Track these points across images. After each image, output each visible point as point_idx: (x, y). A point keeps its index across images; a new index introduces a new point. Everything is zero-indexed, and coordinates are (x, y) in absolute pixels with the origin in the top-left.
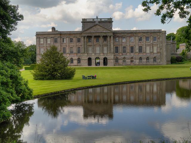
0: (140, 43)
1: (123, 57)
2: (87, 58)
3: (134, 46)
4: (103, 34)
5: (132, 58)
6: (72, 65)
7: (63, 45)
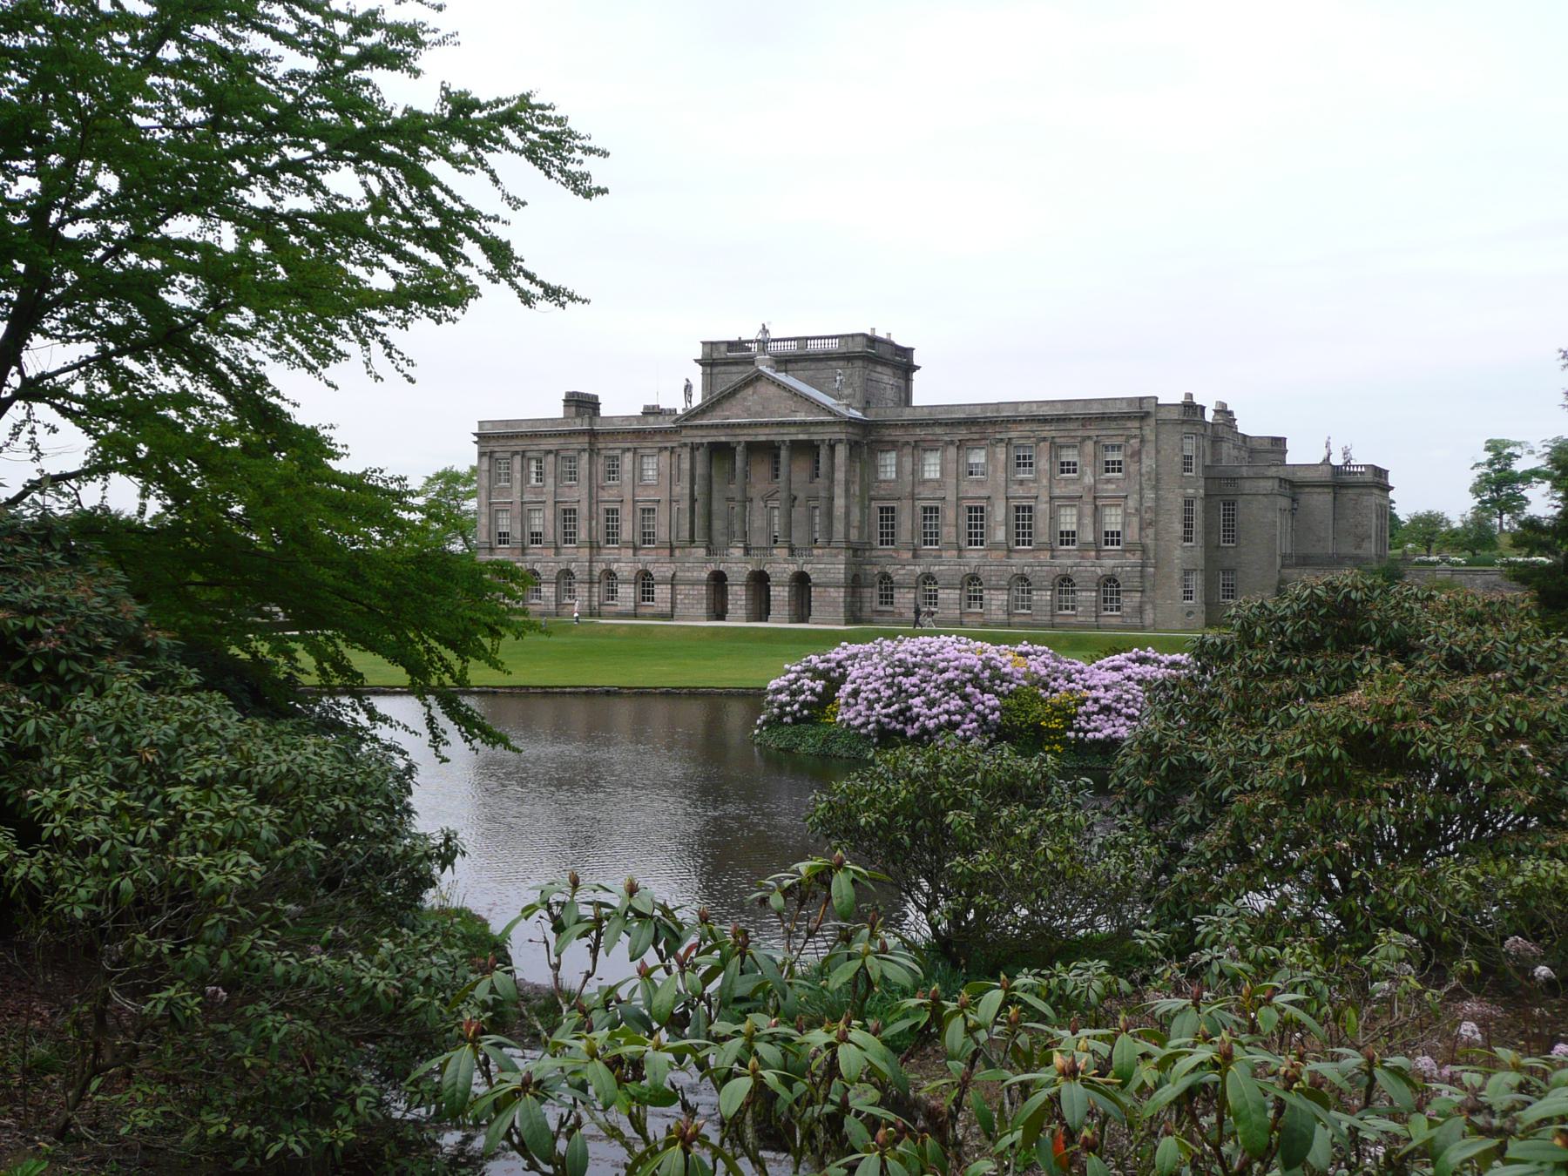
0: (1021, 482)
1: (919, 570)
2: (705, 575)
3: (983, 503)
4: (793, 430)
5: (973, 579)
6: (649, 610)
7: (604, 495)
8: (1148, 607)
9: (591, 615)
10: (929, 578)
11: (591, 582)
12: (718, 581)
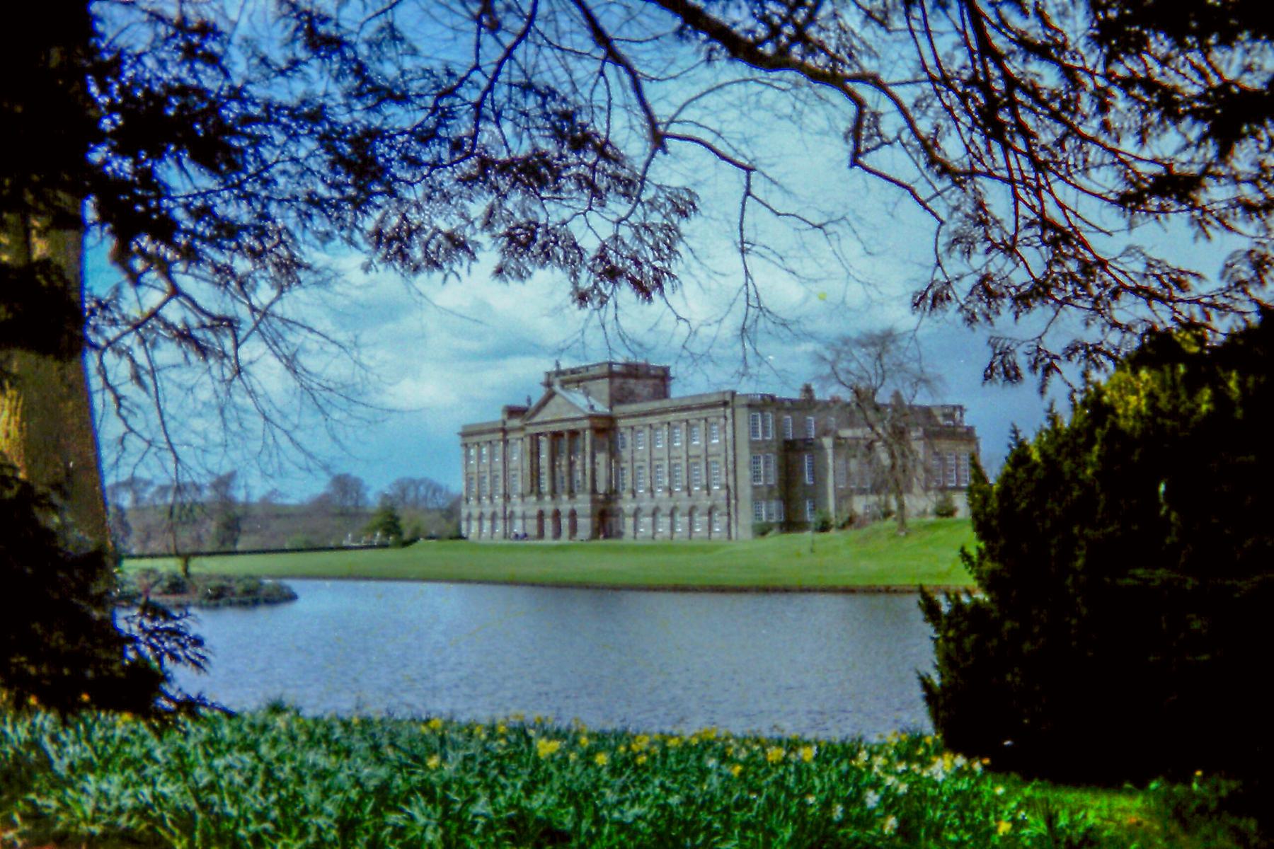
8: (733, 525)
12: (541, 516)
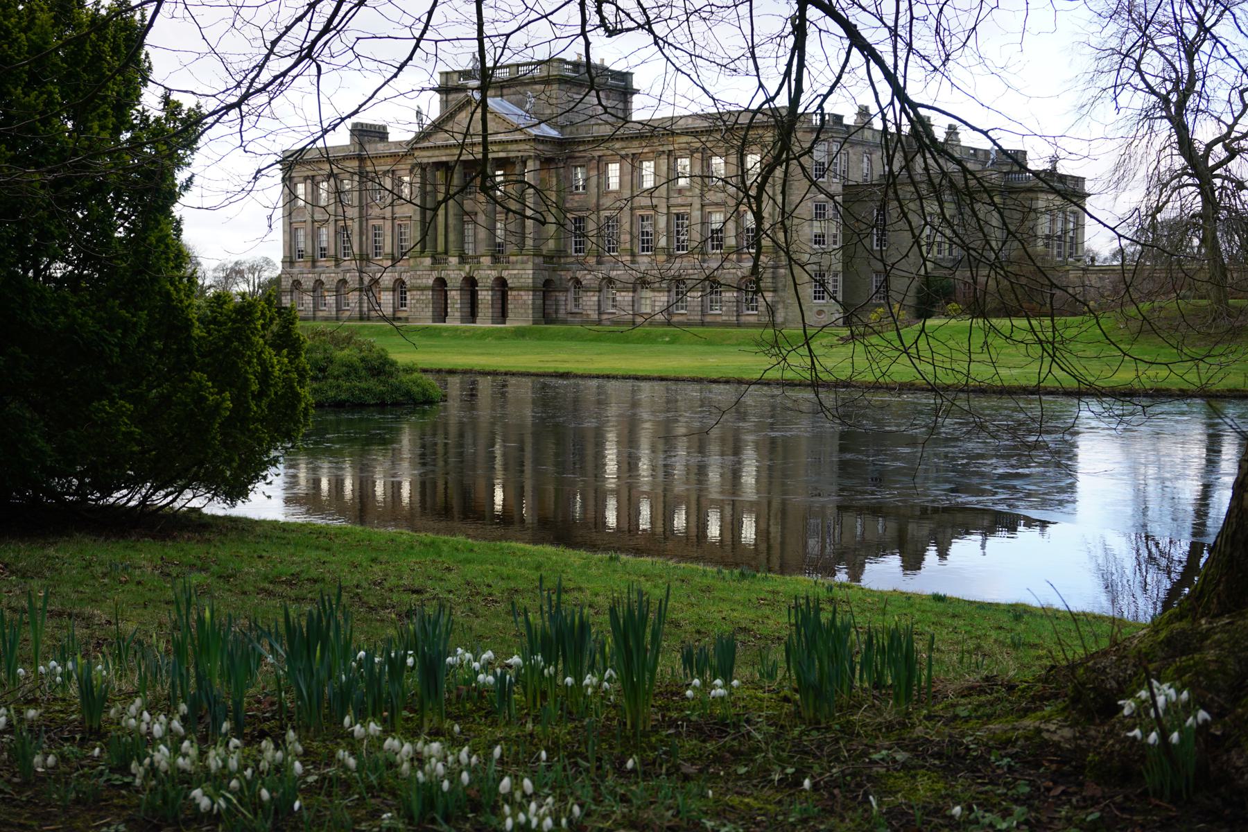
2: (431, 282)
9: (361, 319)
10: (610, 281)
11: (361, 290)
